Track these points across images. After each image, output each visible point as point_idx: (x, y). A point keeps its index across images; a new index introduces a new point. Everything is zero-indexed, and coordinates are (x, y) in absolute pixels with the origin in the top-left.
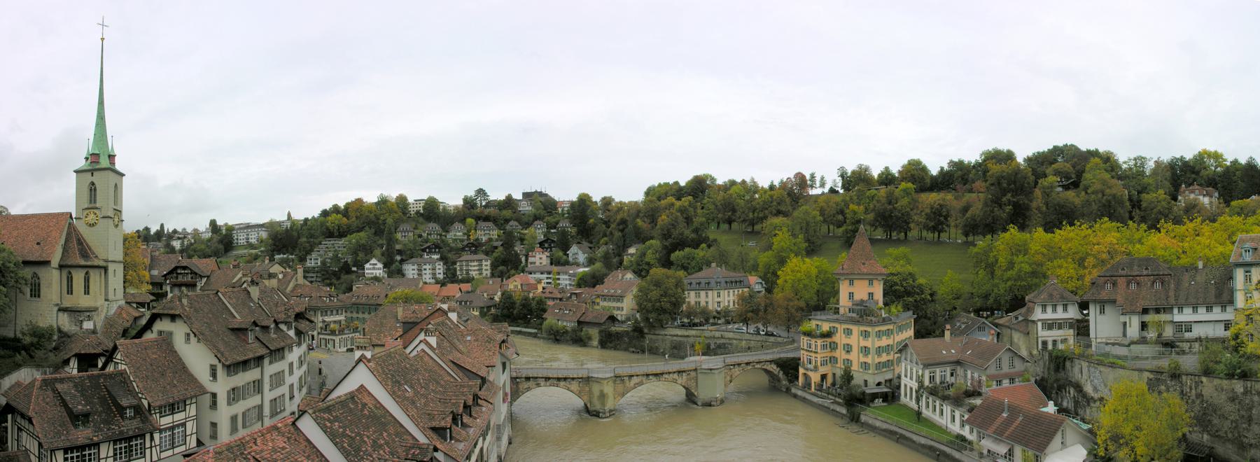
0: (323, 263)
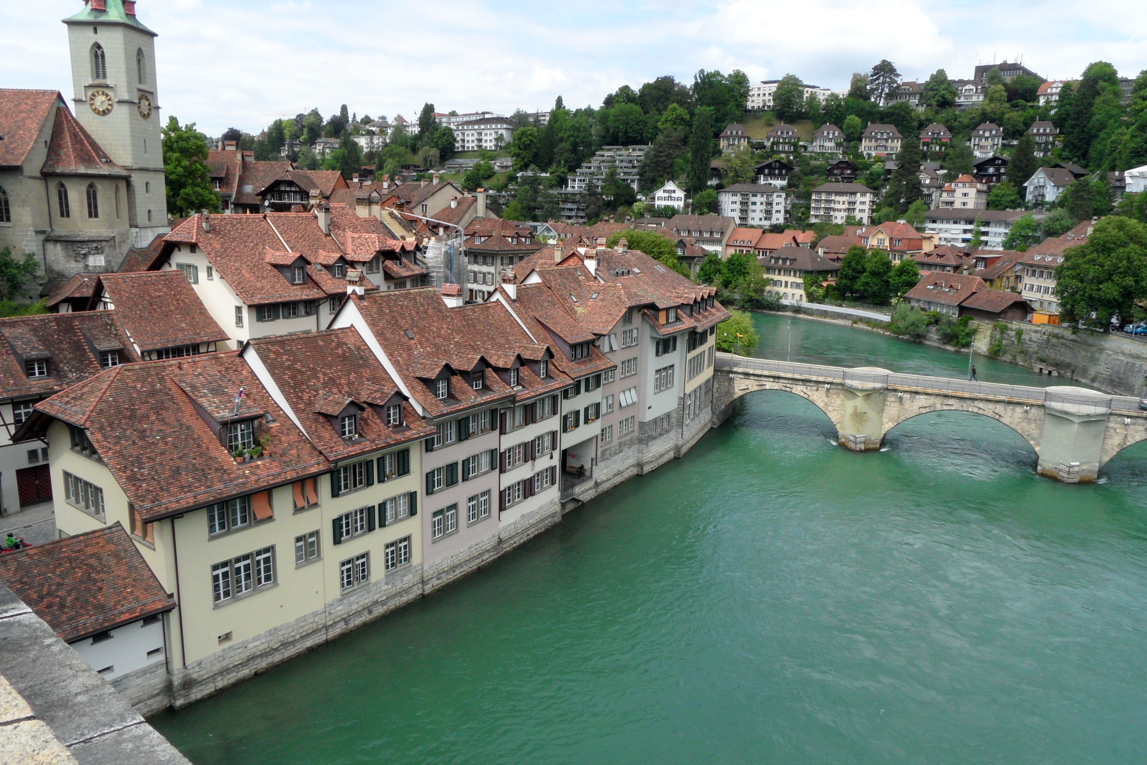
0: (591, 187)
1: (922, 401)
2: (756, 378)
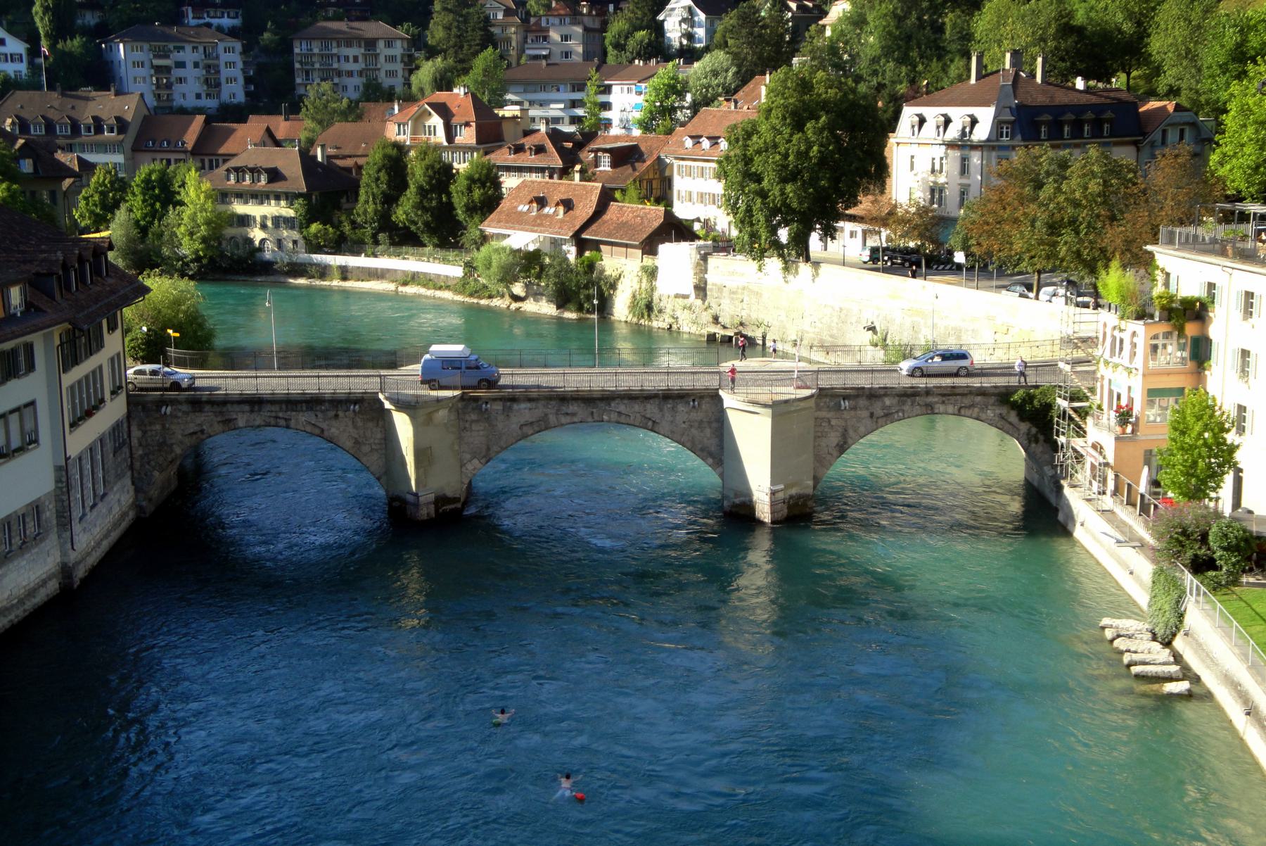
2: (217, 409)
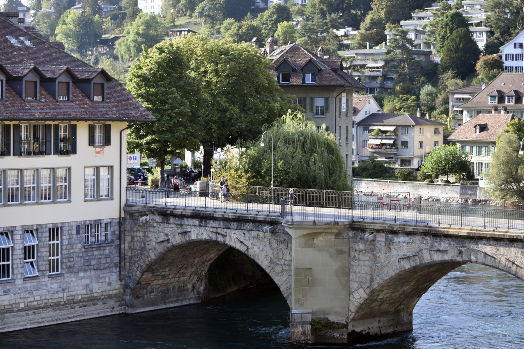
1: (404, 246)
